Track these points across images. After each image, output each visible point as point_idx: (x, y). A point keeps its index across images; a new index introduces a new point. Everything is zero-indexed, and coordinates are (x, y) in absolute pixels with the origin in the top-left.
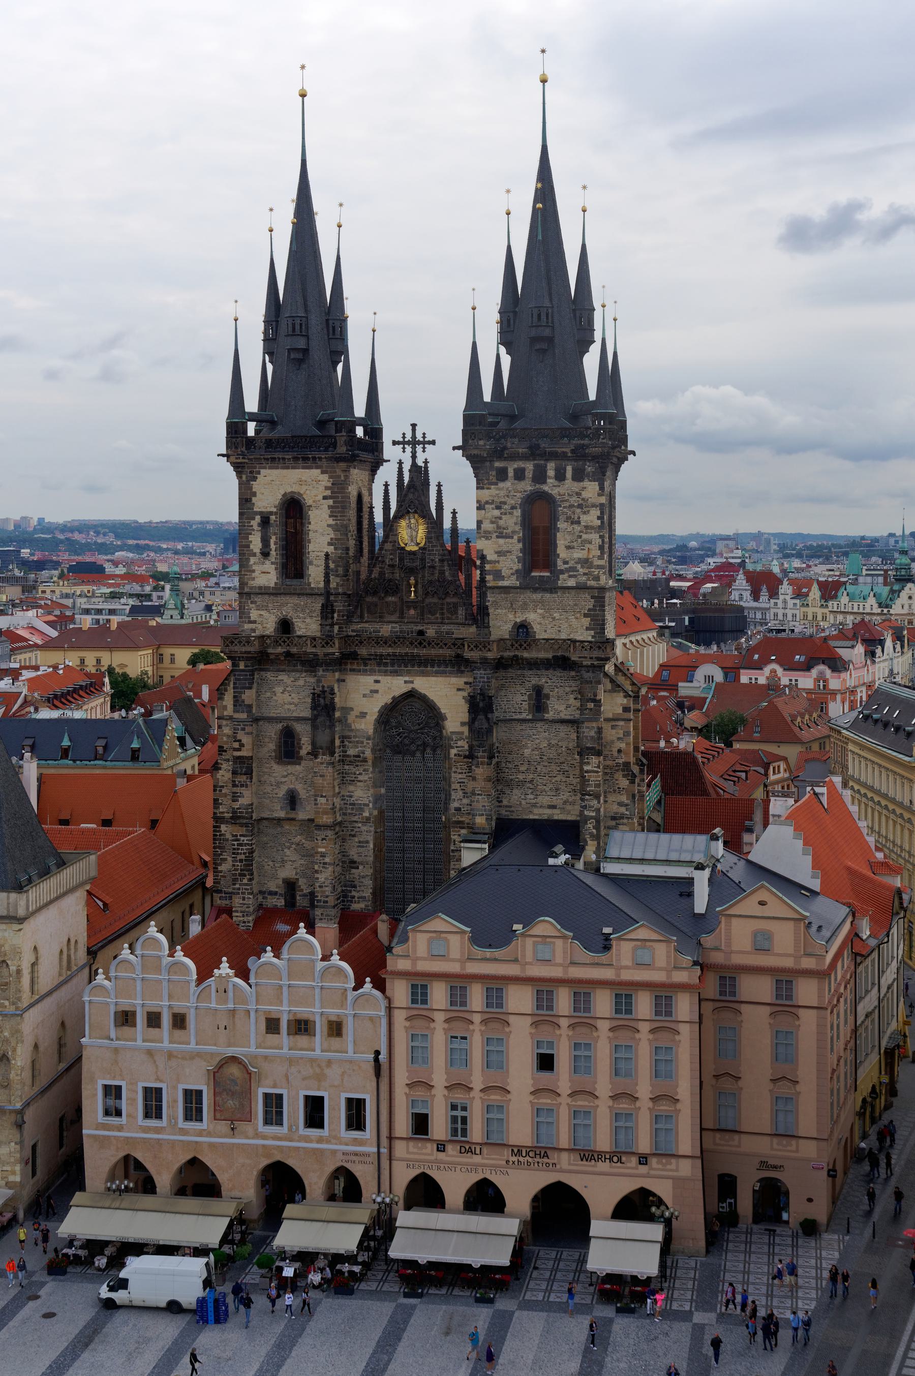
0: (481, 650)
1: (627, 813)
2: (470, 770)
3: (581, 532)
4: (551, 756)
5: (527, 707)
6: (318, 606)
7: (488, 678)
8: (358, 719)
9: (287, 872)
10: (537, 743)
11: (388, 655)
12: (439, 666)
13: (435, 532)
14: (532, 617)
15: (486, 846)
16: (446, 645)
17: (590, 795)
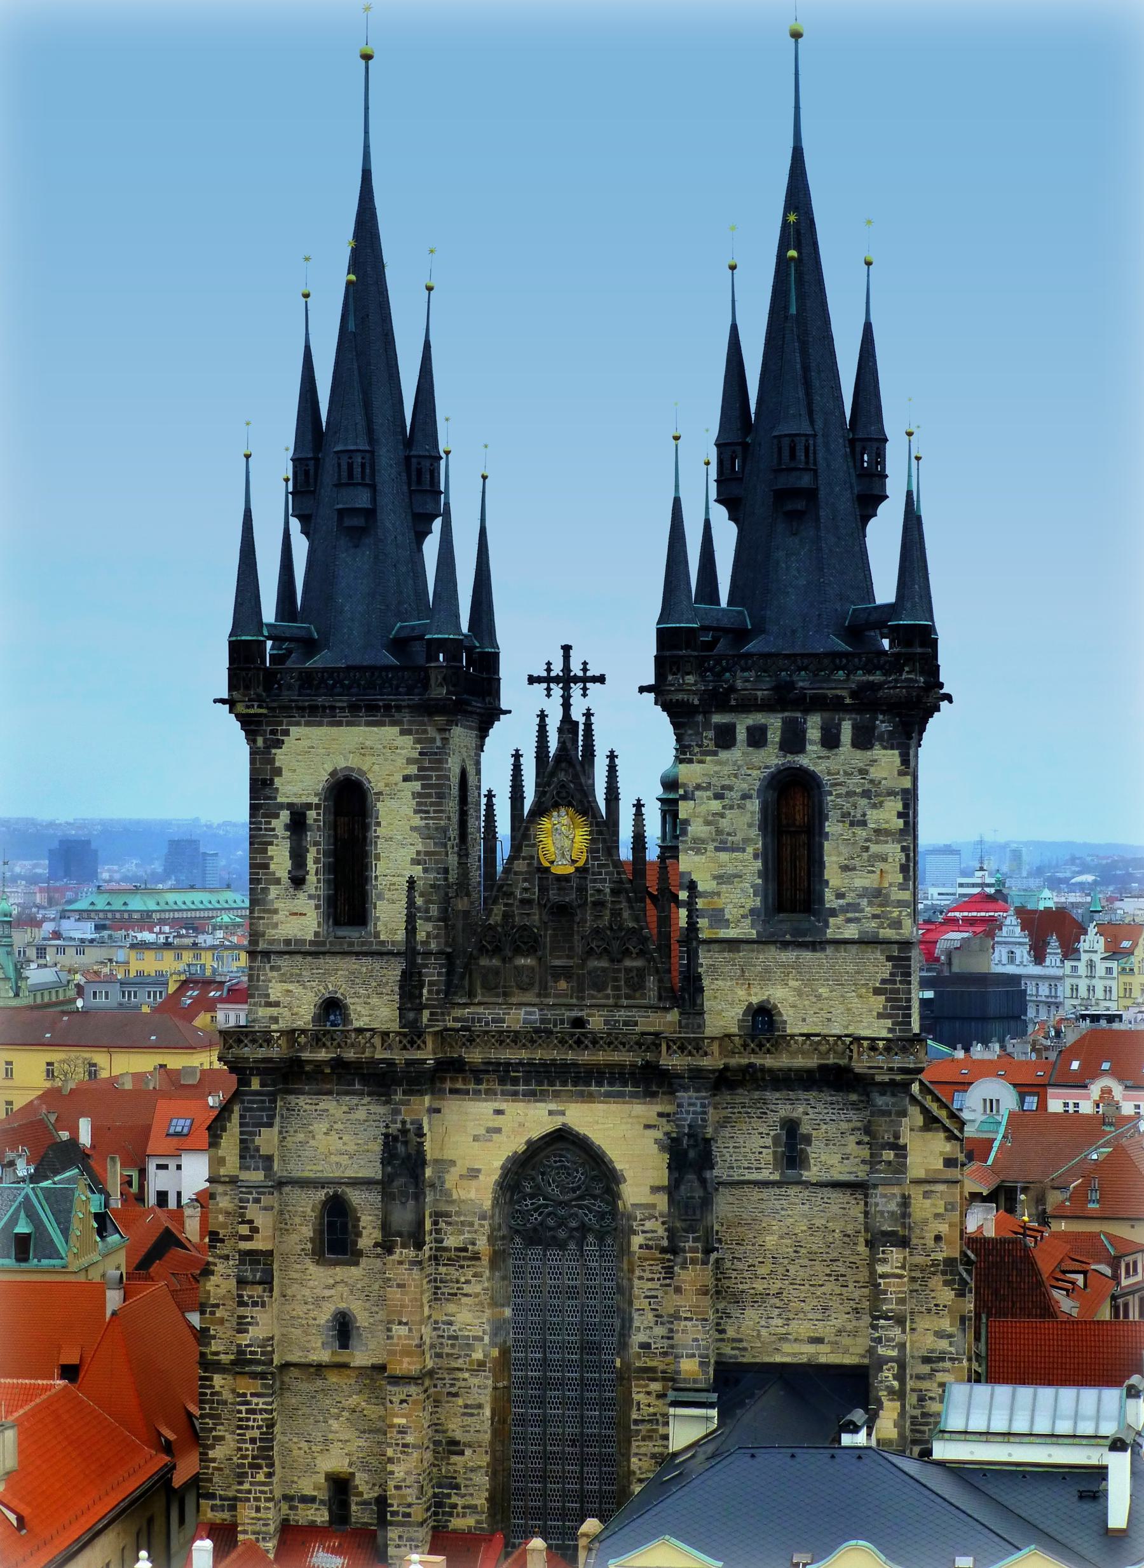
0: (690, 1054)
1: (953, 1349)
2: (669, 1272)
3: (867, 840)
4: (815, 1248)
5: (770, 1158)
6: (394, 972)
7: (703, 1106)
8: (465, 1182)
9: (335, 1462)
10: (785, 1227)
11: (521, 1064)
12: (611, 1084)
13: (604, 841)
14: (780, 995)
15: (714, 1413)
16: (624, 1044)
17: (887, 1318)
